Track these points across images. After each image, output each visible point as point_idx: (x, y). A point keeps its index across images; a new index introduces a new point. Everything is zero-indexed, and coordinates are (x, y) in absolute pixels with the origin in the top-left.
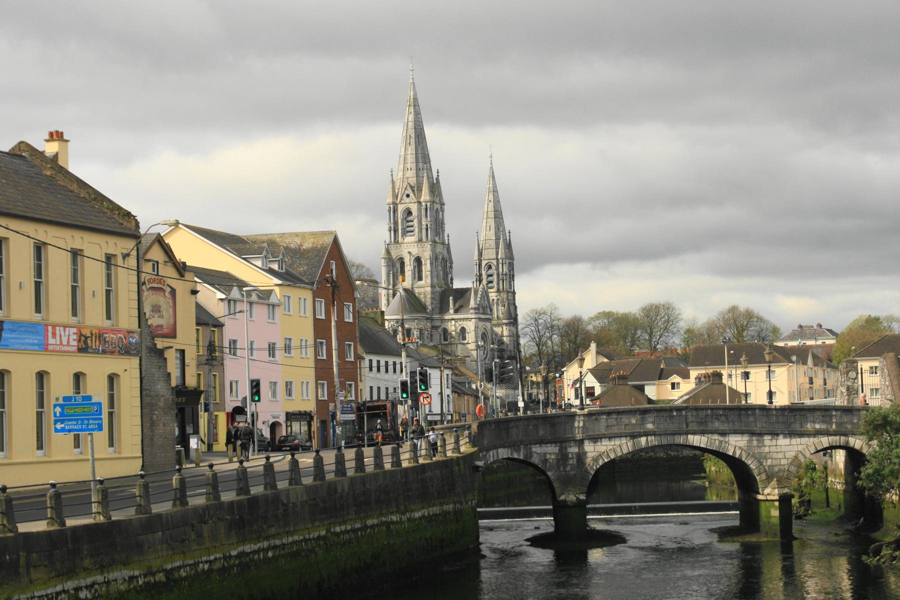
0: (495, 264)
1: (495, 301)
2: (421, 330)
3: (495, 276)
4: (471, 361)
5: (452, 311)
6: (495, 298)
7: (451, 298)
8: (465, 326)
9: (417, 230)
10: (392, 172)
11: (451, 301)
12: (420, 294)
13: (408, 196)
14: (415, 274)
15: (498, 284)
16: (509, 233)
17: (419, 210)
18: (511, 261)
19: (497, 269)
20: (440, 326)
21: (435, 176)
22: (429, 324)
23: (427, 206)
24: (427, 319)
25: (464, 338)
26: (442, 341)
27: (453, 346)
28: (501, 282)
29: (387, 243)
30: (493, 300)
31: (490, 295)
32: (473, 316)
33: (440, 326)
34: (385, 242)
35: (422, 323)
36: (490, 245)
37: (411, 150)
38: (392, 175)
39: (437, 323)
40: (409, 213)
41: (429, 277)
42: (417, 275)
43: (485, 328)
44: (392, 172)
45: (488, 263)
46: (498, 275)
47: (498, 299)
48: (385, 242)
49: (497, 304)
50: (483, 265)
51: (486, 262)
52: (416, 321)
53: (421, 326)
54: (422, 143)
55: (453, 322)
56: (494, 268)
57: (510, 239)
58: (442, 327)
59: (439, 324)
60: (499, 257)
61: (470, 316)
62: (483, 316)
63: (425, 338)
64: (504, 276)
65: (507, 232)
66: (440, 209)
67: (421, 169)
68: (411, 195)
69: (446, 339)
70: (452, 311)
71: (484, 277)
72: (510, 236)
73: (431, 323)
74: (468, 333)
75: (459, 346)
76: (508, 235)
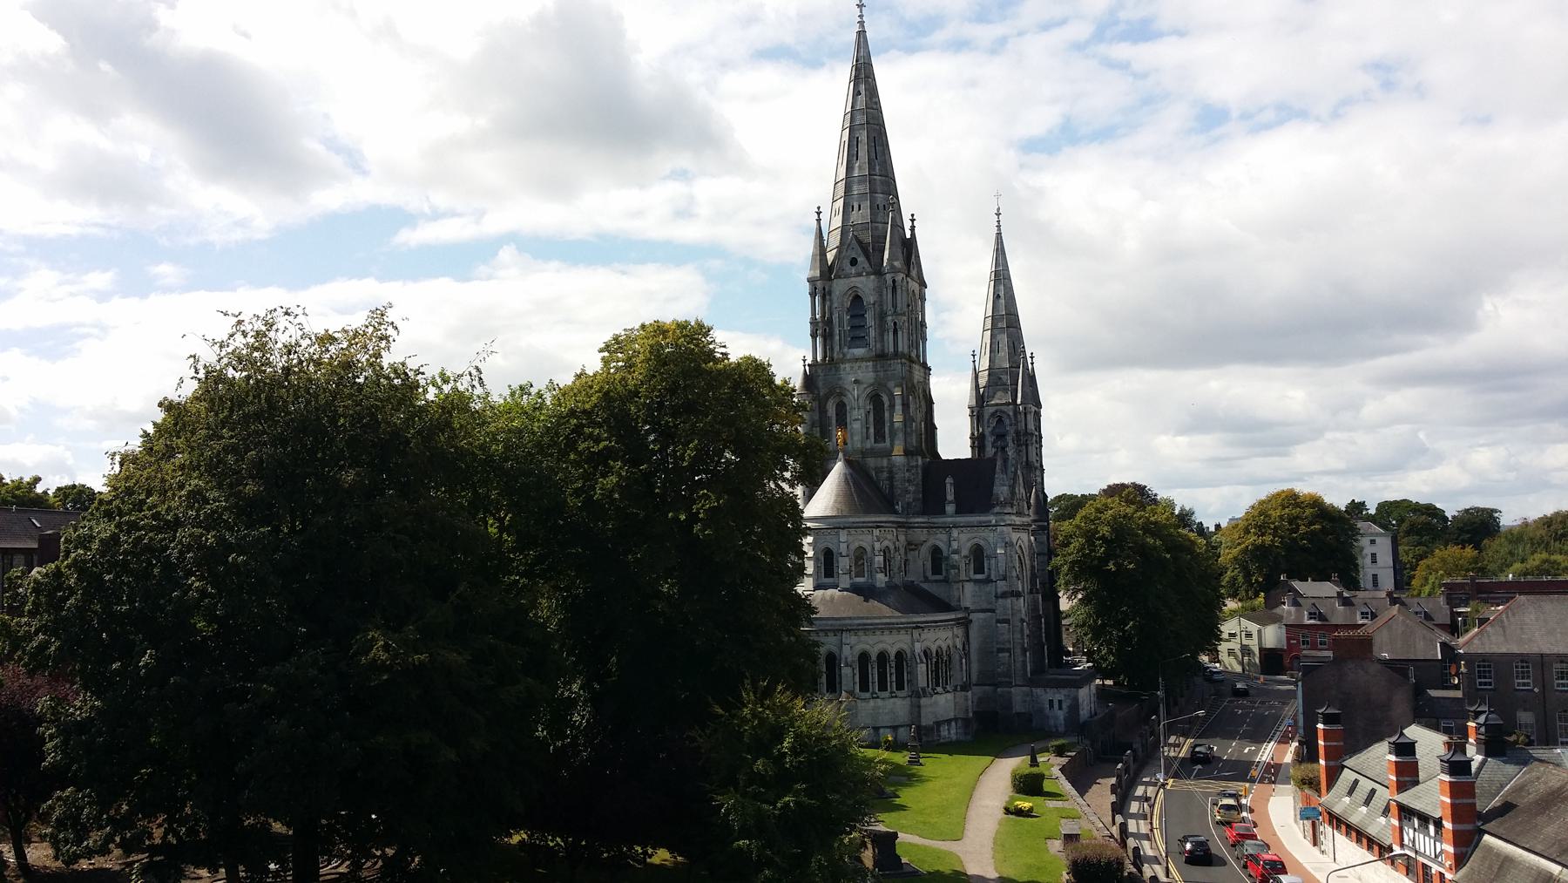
0: (1011, 414)
2: (886, 551)
4: (998, 621)
5: (950, 508)
7: (949, 480)
8: (982, 543)
9: (872, 333)
10: (819, 213)
11: (948, 486)
12: (879, 470)
13: (854, 262)
14: (868, 428)
17: (879, 291)
18: (1036, 409)
21: (907, 225)
22: (902, 538)
23: (894, 281)
24: (900, 525)
25: (979, 569)
26: (929, 574)
27: (955, 586)
29: (809, 361)
34: (804, 361)
35: (890, 537)
37: (860, 167)
38: (819, 220)
39: (920, 535)
40: (857, 299)
41: (901, 435)
42: (872, 430)
43: (1020, 546)
44: (819, 213)
45: (996, 411)
48: (804, 361)
50: (986, 417)
51: (992, 410)
52: (876, 532)
53: (886, 543)
54: (884, 154)
55: (955, 533)
57: (1033, 369)
58: (929, 544)
59: (923, 538)
60: (1019, 401)
62: (1018, 520)
63: (896, 570)
65: (1028, 355)
66: (917, 292)
67: (881, 207)
68: (861, 259)
69: (936, 569)
70: (950, 508)
71: (990, 440)
72: (1032, 364)
74: (989, 558)
75: (969, 587)
76: (1029, 360)
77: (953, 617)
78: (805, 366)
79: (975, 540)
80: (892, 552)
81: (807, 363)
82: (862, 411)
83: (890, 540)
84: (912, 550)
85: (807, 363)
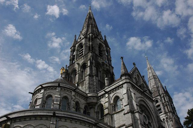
0: (159, 98)
1: (165, 120)
3: (161, 106)
6: (165, 118)
15: (164, 109)
16: (165, 87)
19: (161, 101)
20: (97, 103)
28: (166, 107)
30: (164, 119)
31: (161, 117)
32: (124, 81)
33: (97, 103)
34: (66, 66)
35: (67, 93)
36: (154, 90)
46: (163, 104)
47: (167, 118)
49: (167, 121)
52: (58, 89)
56: (159, 101)
59: (95, 101)
61: (121, 83)
64: (167, 103)
73: (86, 100)
76: (165, 88)
77: (94, 121)
78: (66, 67)
79: (116, 94)
80: (70, 100)
81: (67, 67)
82: (80, 71)
83: (67, 94)
84: (91, 108)
85: (67, 67)
